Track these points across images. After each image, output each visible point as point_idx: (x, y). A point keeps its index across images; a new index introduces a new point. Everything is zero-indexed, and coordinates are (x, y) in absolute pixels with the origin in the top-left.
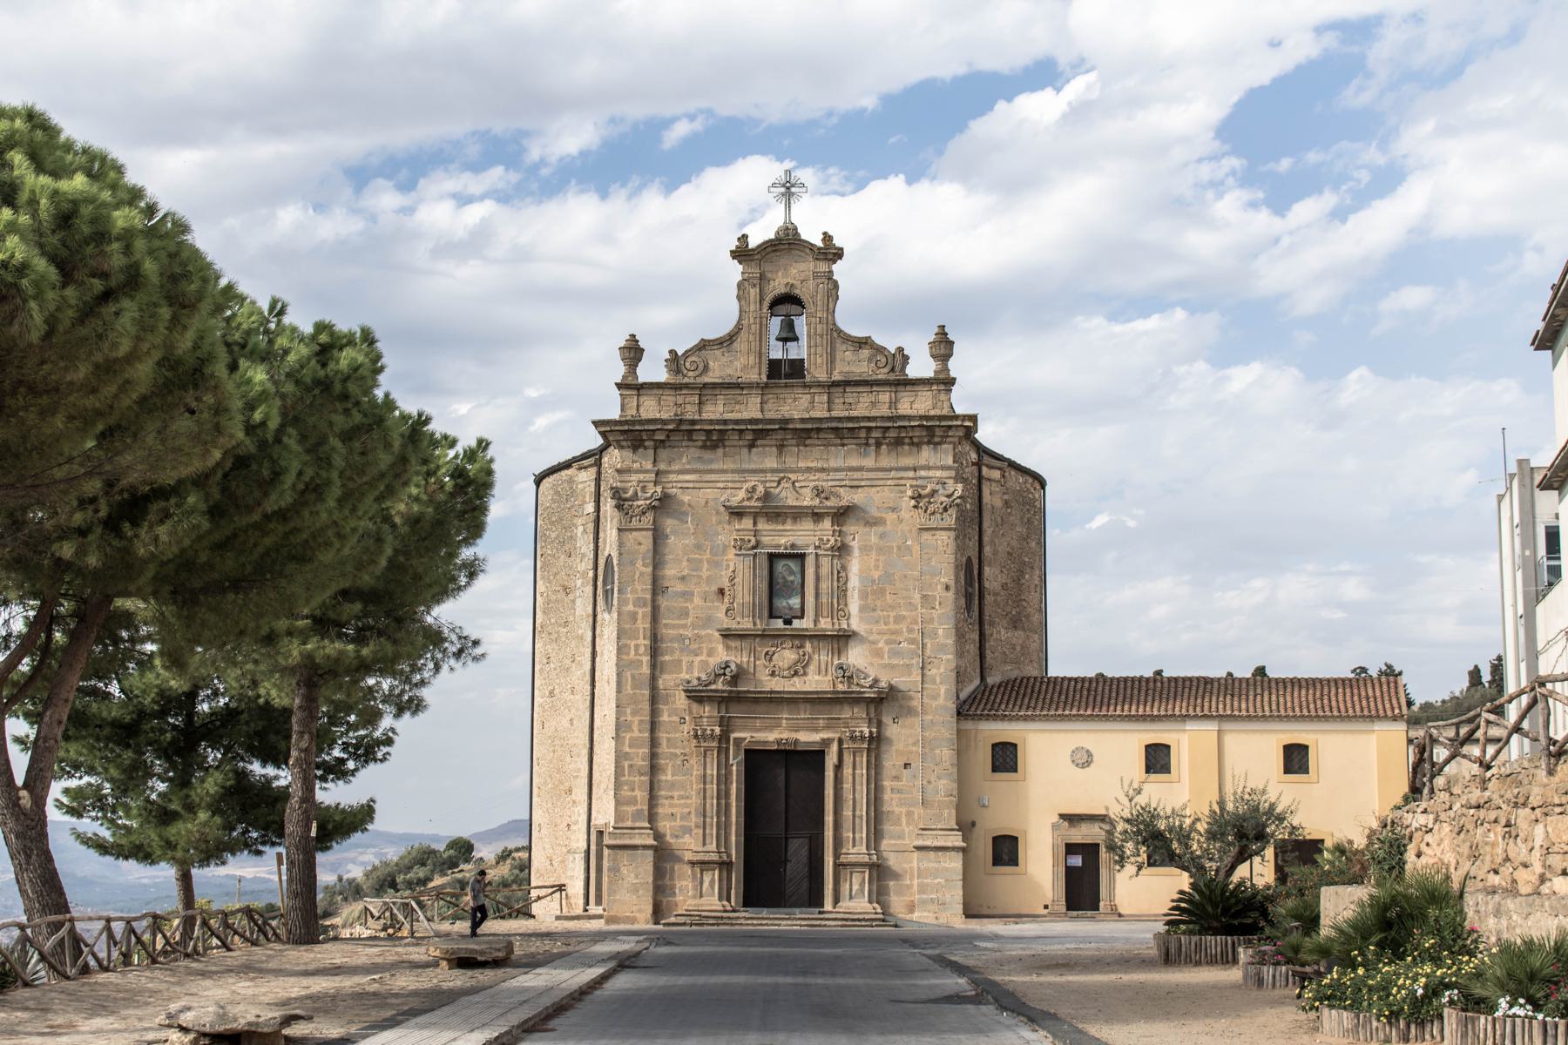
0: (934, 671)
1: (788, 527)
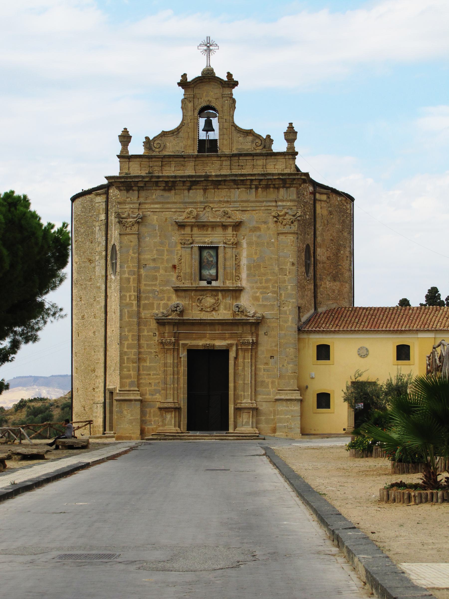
0: (286, 308)
1: (209, 233)
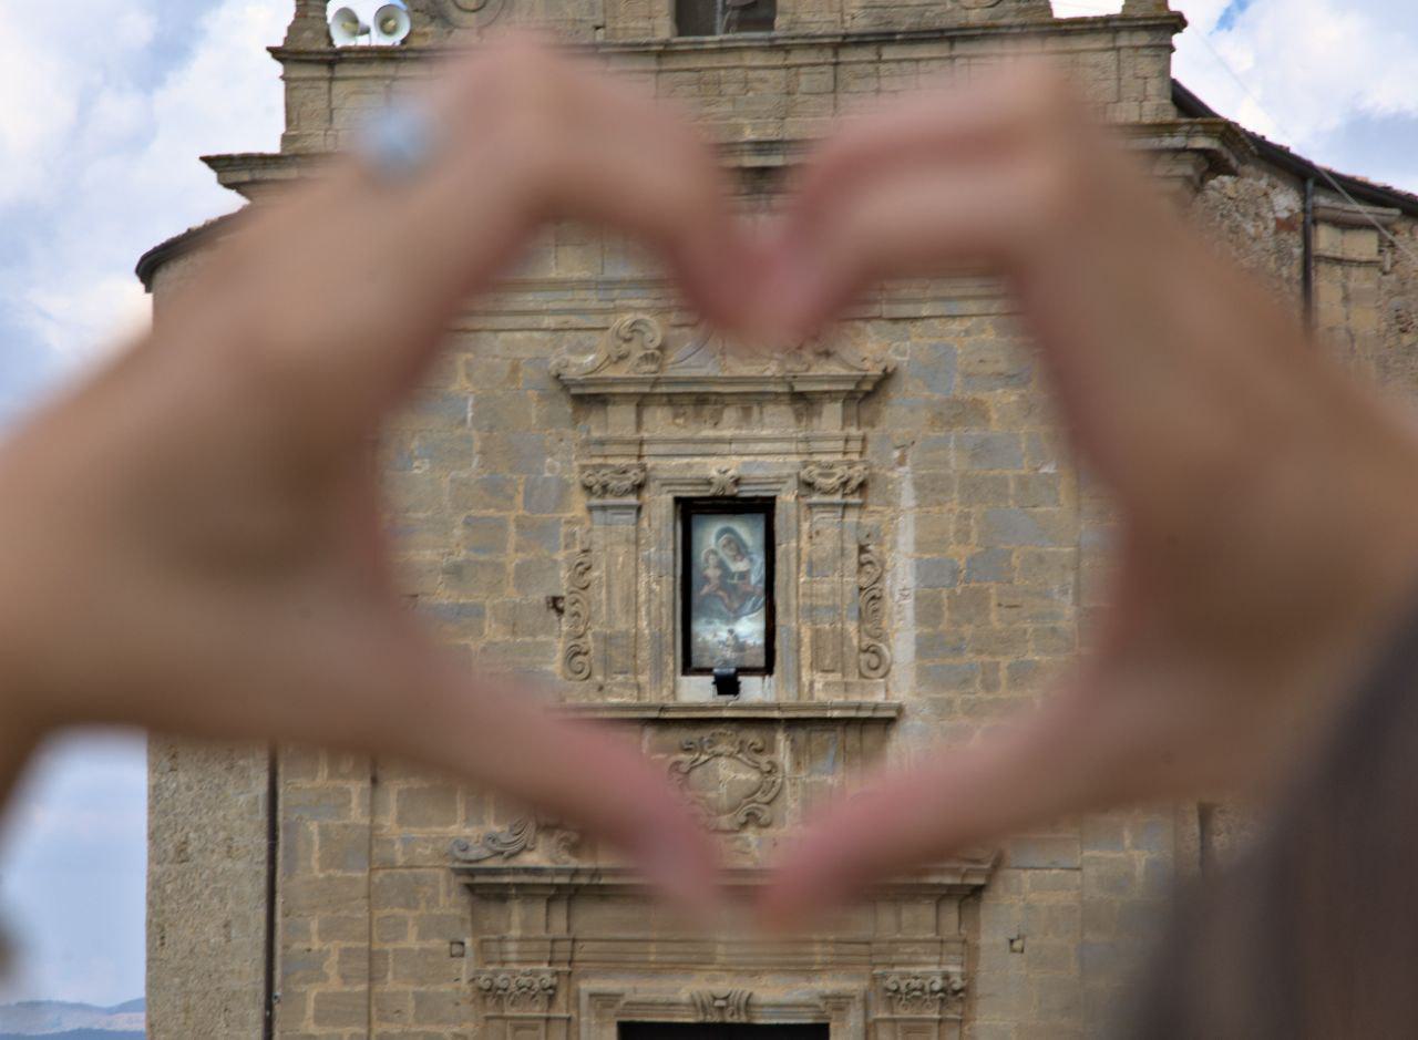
1: (728, 433)
